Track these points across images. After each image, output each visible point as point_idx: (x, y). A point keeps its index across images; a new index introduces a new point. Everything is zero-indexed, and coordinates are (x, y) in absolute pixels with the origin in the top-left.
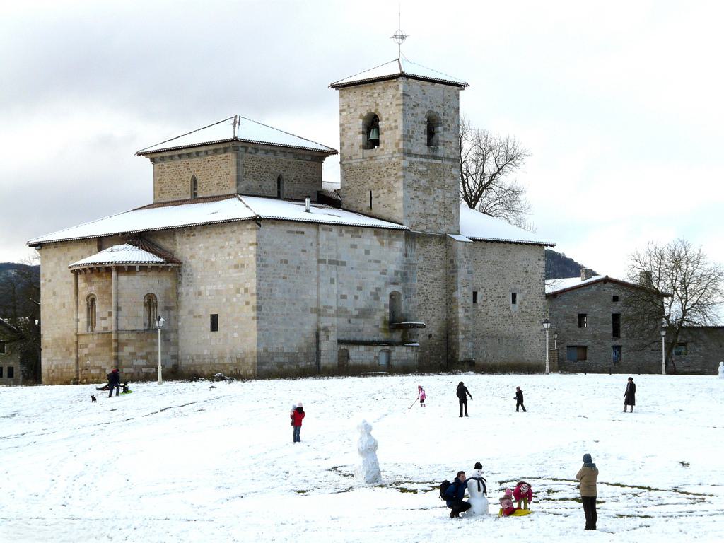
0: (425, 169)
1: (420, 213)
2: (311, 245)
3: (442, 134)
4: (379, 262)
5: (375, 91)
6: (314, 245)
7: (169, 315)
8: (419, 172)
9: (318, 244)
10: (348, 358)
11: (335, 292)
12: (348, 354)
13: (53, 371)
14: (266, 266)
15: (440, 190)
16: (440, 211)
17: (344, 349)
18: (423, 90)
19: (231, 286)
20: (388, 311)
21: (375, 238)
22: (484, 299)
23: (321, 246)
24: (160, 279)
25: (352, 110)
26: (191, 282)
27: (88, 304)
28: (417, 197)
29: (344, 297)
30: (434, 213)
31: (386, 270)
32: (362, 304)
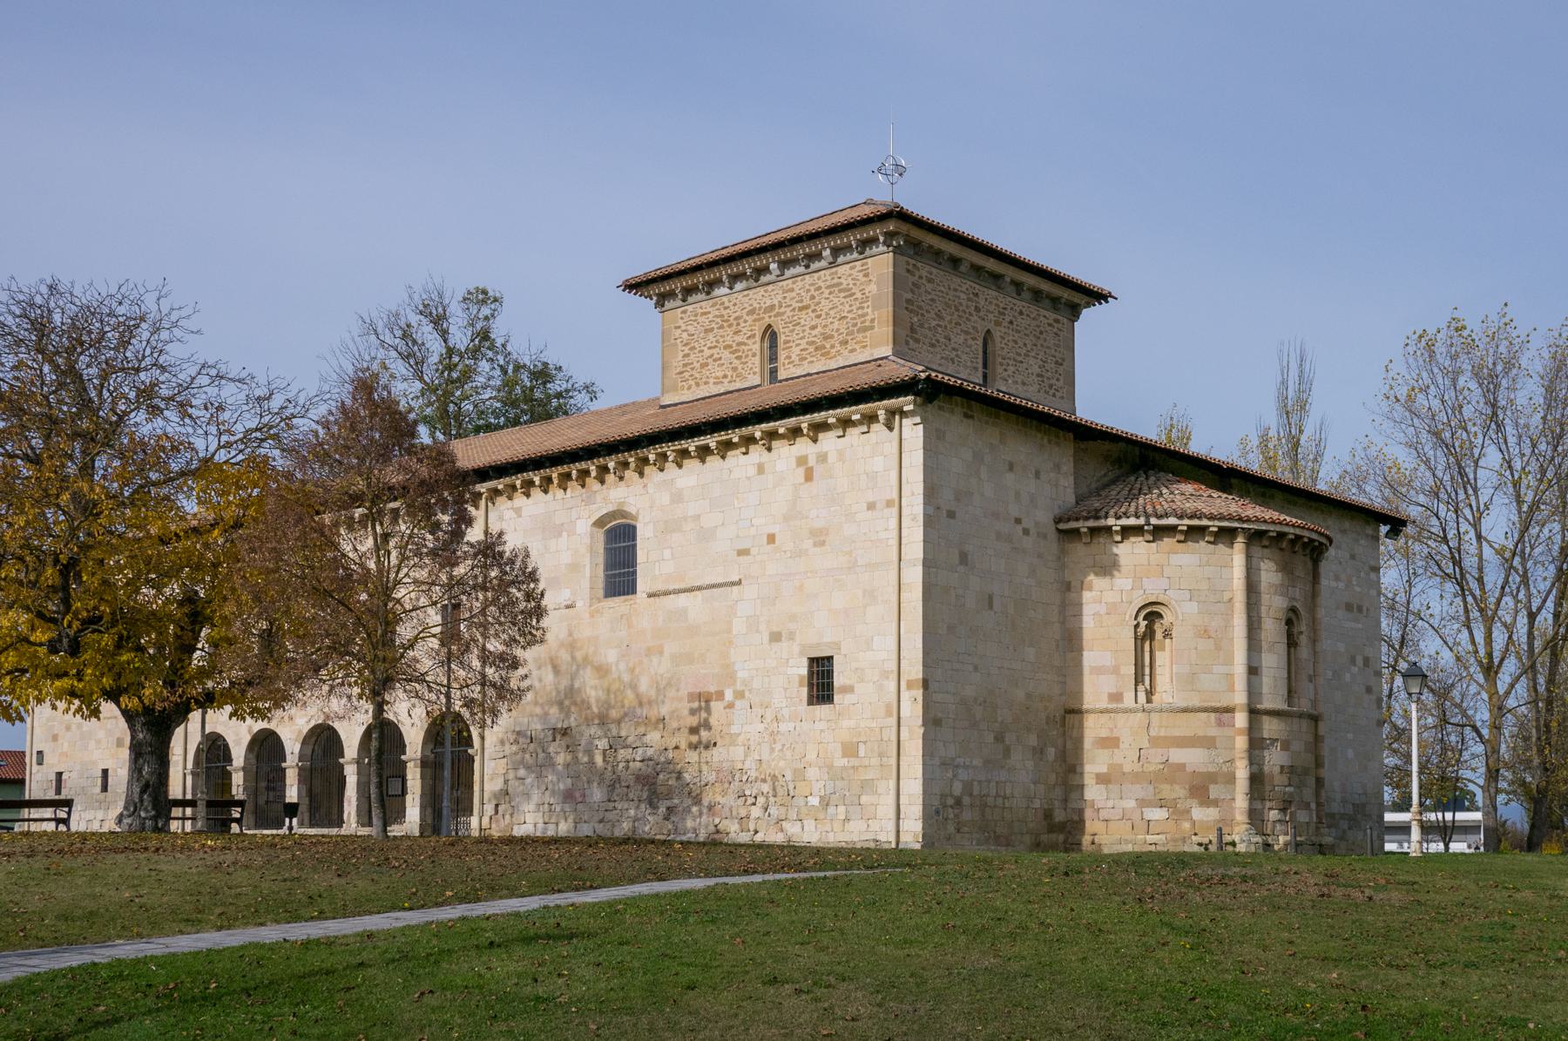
19: (1341, 647)
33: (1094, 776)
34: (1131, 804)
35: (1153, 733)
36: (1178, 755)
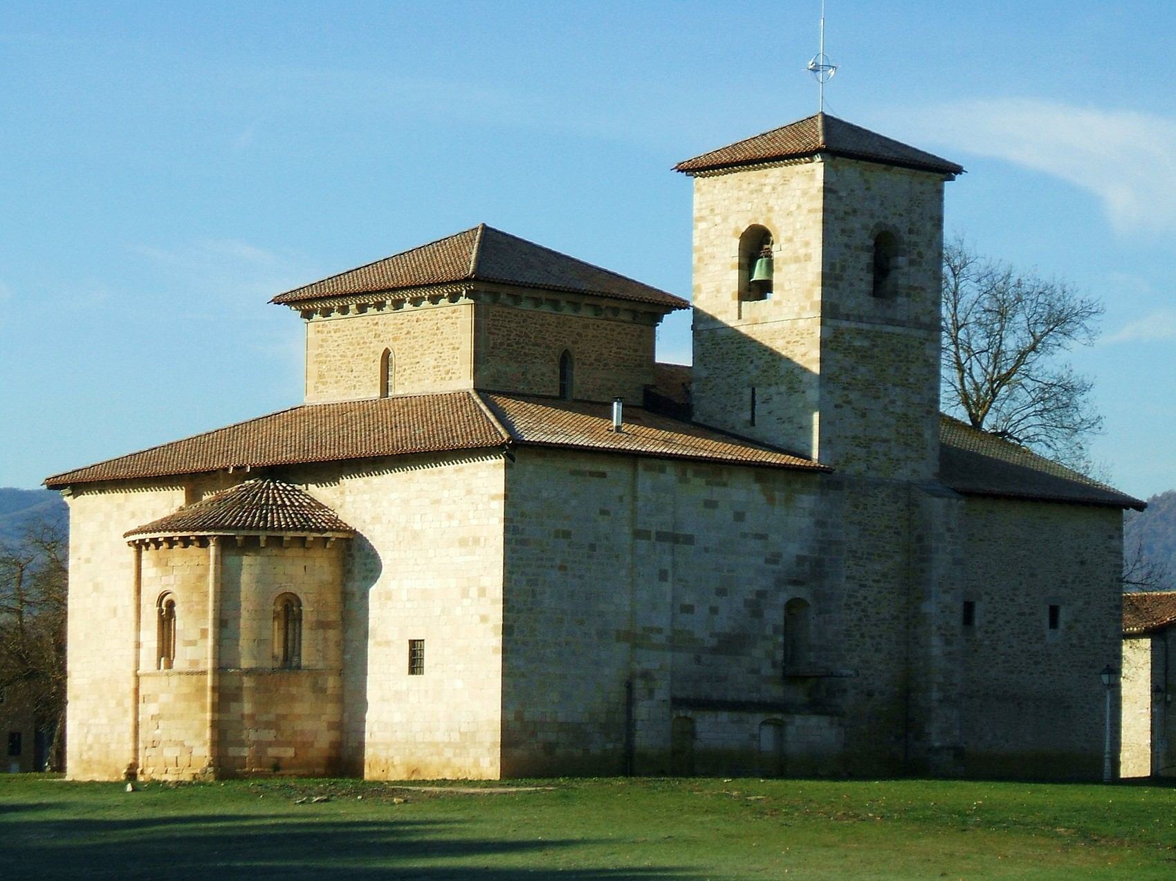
0: (866, 343)
1: (854, 438)
2: (621, 499)
3: (904, 272)
4: (761, 537)
5: (767, 181)
6: (627, 499)
7: (325, 639)
8: (855, 350)
9: (635, 498)
10: (693, 734)
11: (669, 599)
12: (694, 728)
13: (90, 748)
14: (523, 542)
15: (898, 389)
16: (898, 433)
17: (686, 717)
18: (866, 181)
20: (781, 639)
21: (757, 487)
22: (990, 617)
23: (640, 504)
24: (309, 563)
25: (718, 219)
26: (372, 571)
27: (161, 611)
28: (849, 402)
29: (688, 609)
30: (884, 436)
31: (779, 555)
32: (723, 623)
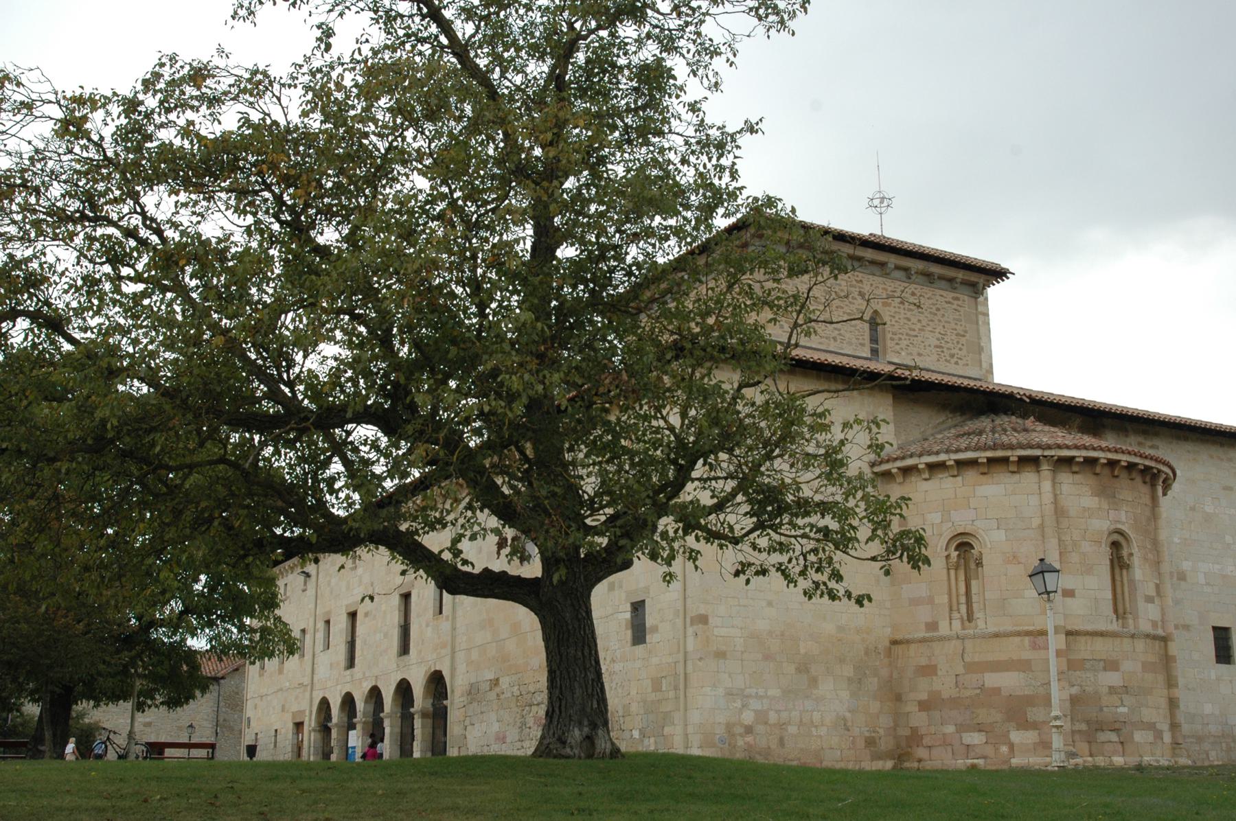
13: (749, 730)
33: (916, 703)
34: (950, 729)
35: (967, 659)
36: (992, 680)
